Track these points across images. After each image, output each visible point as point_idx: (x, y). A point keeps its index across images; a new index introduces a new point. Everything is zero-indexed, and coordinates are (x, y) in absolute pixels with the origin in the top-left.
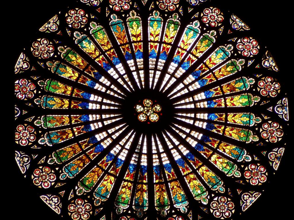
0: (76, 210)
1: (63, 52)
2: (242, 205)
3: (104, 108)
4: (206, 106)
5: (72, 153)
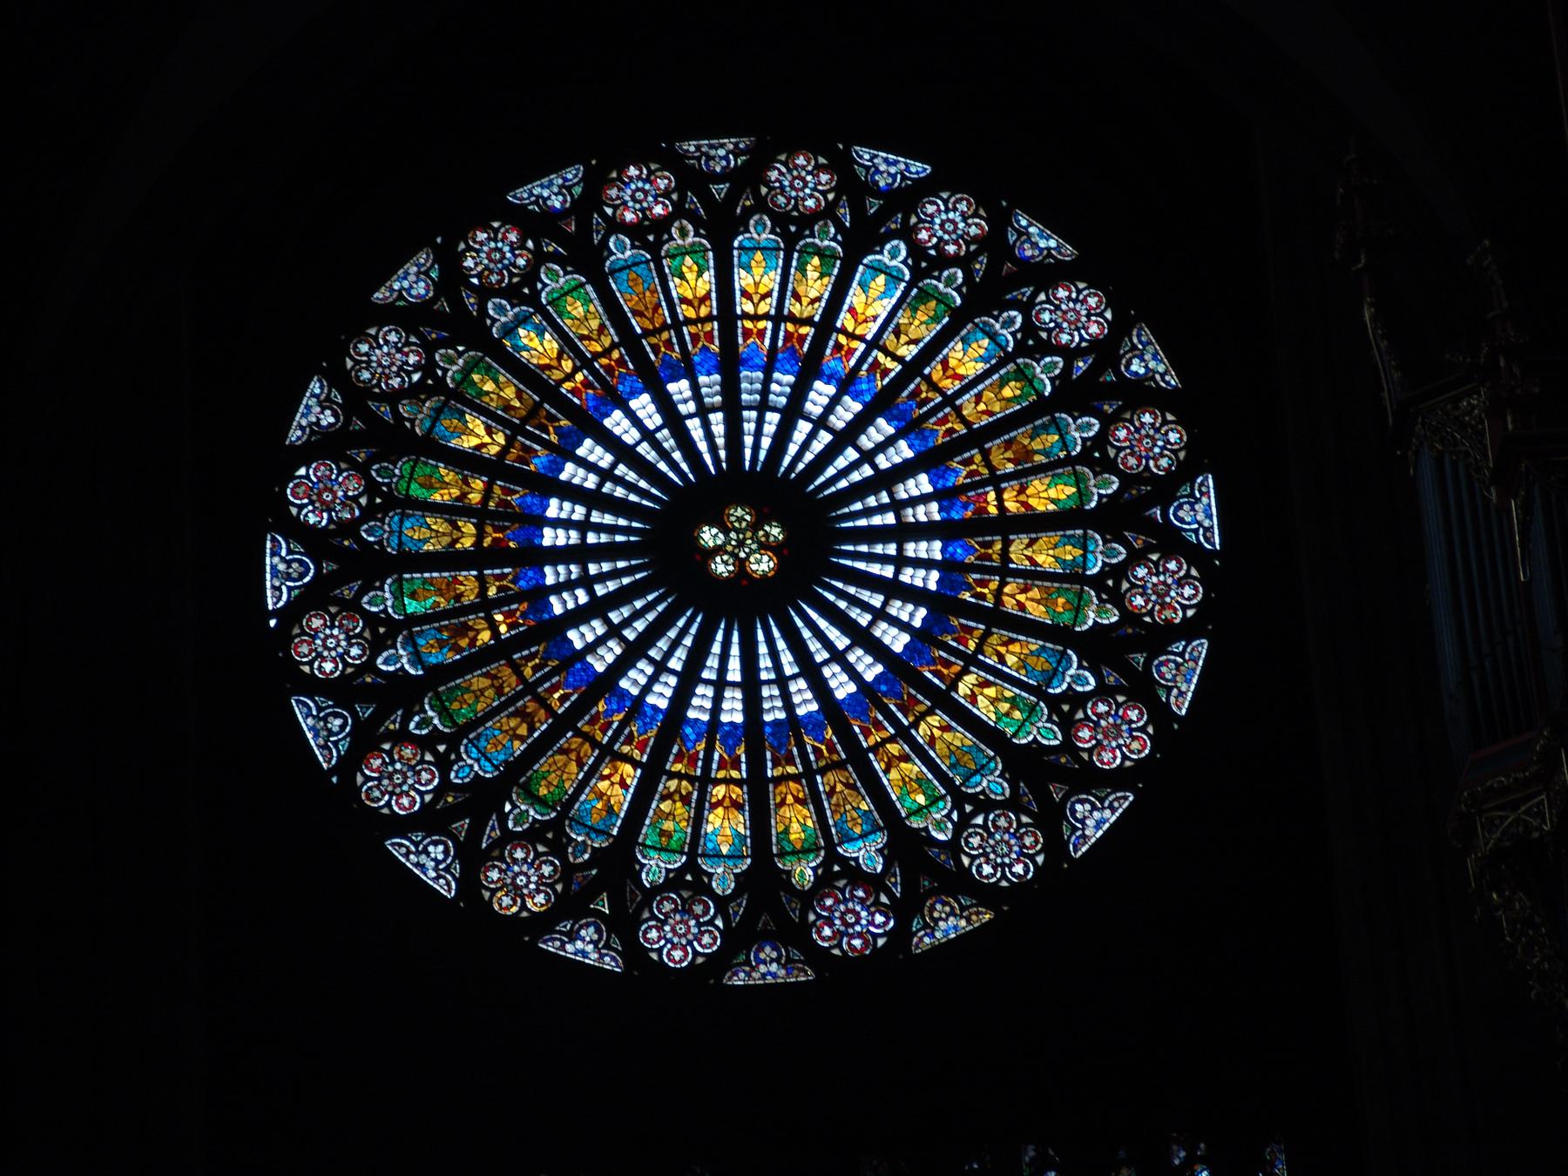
0: (509, 881)
1: (455, 368)
2: (1069, 837)
3: (595, 541)
4: (937, 517)
5: (490, 693)
